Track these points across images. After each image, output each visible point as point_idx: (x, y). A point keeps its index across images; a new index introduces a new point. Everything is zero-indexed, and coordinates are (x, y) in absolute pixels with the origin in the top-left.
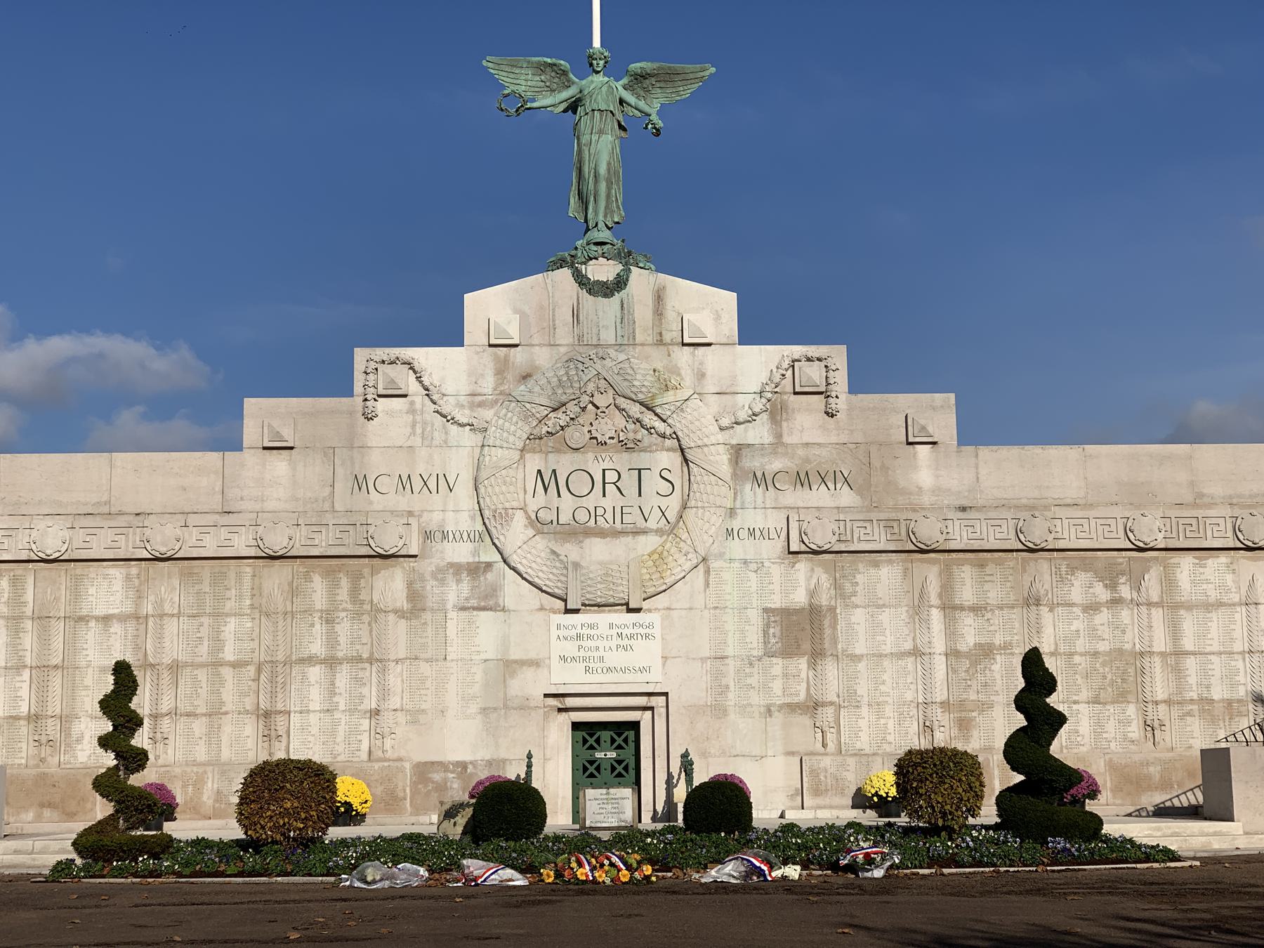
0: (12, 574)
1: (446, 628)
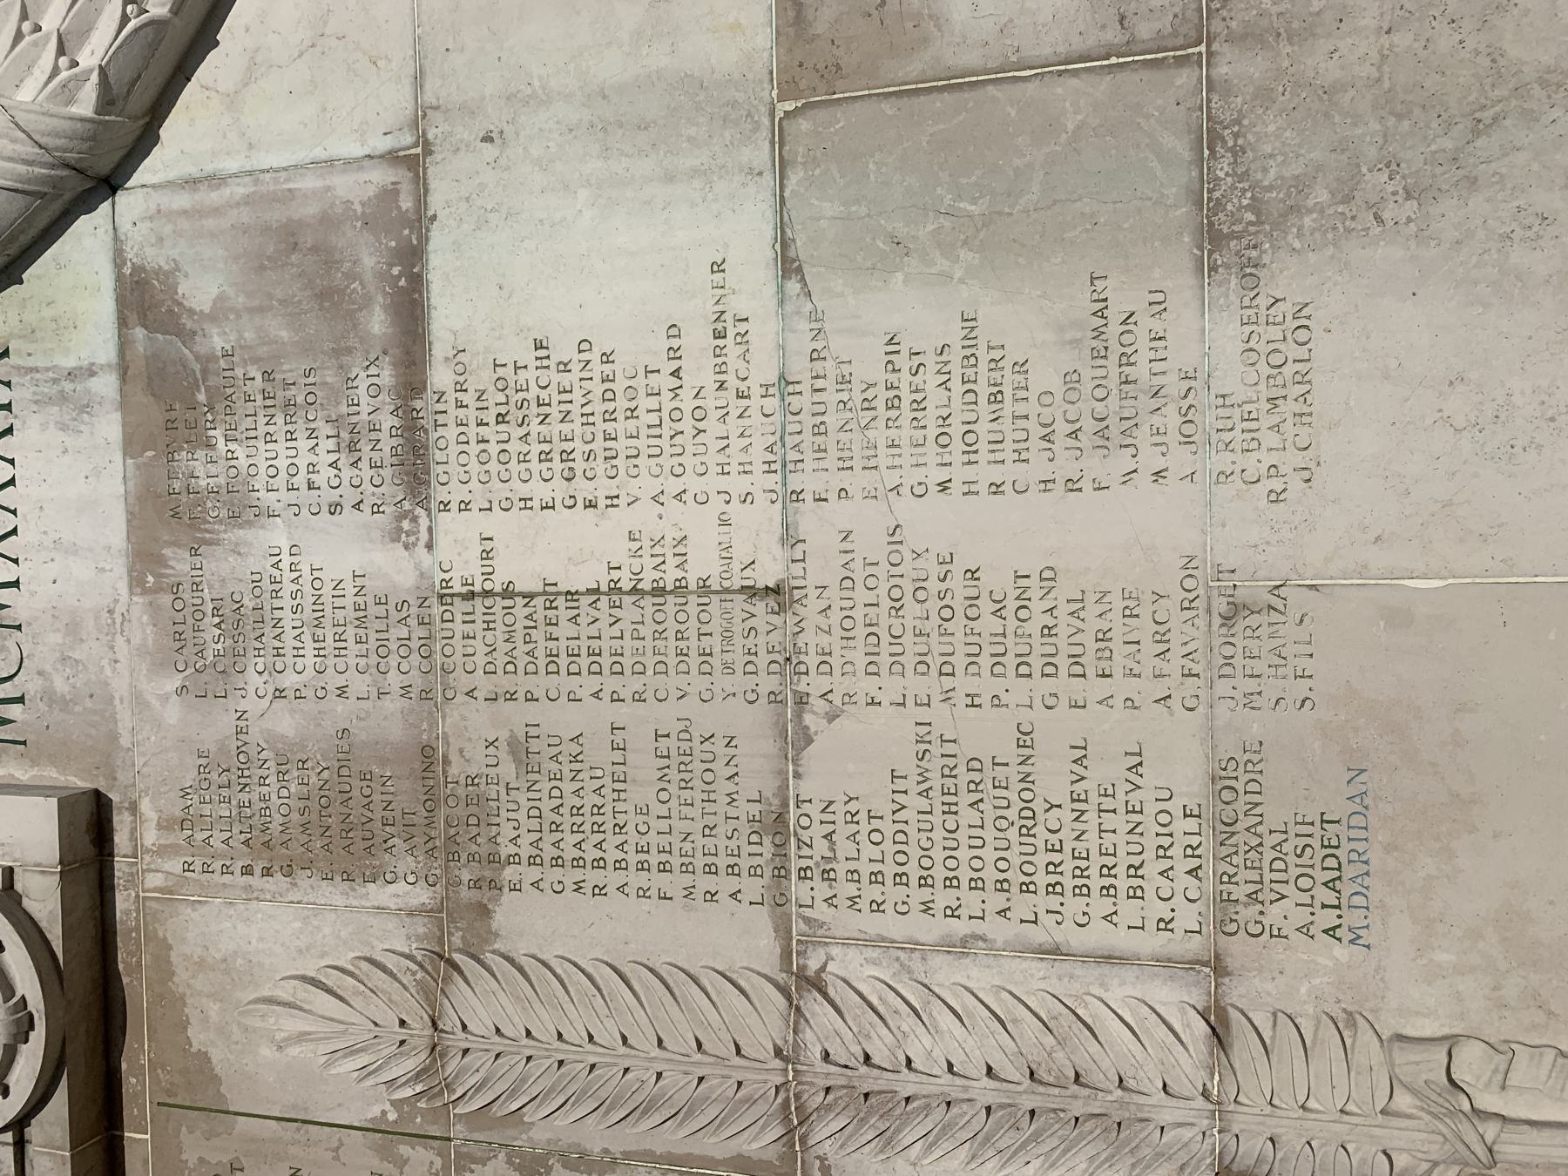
1: (550, 593)
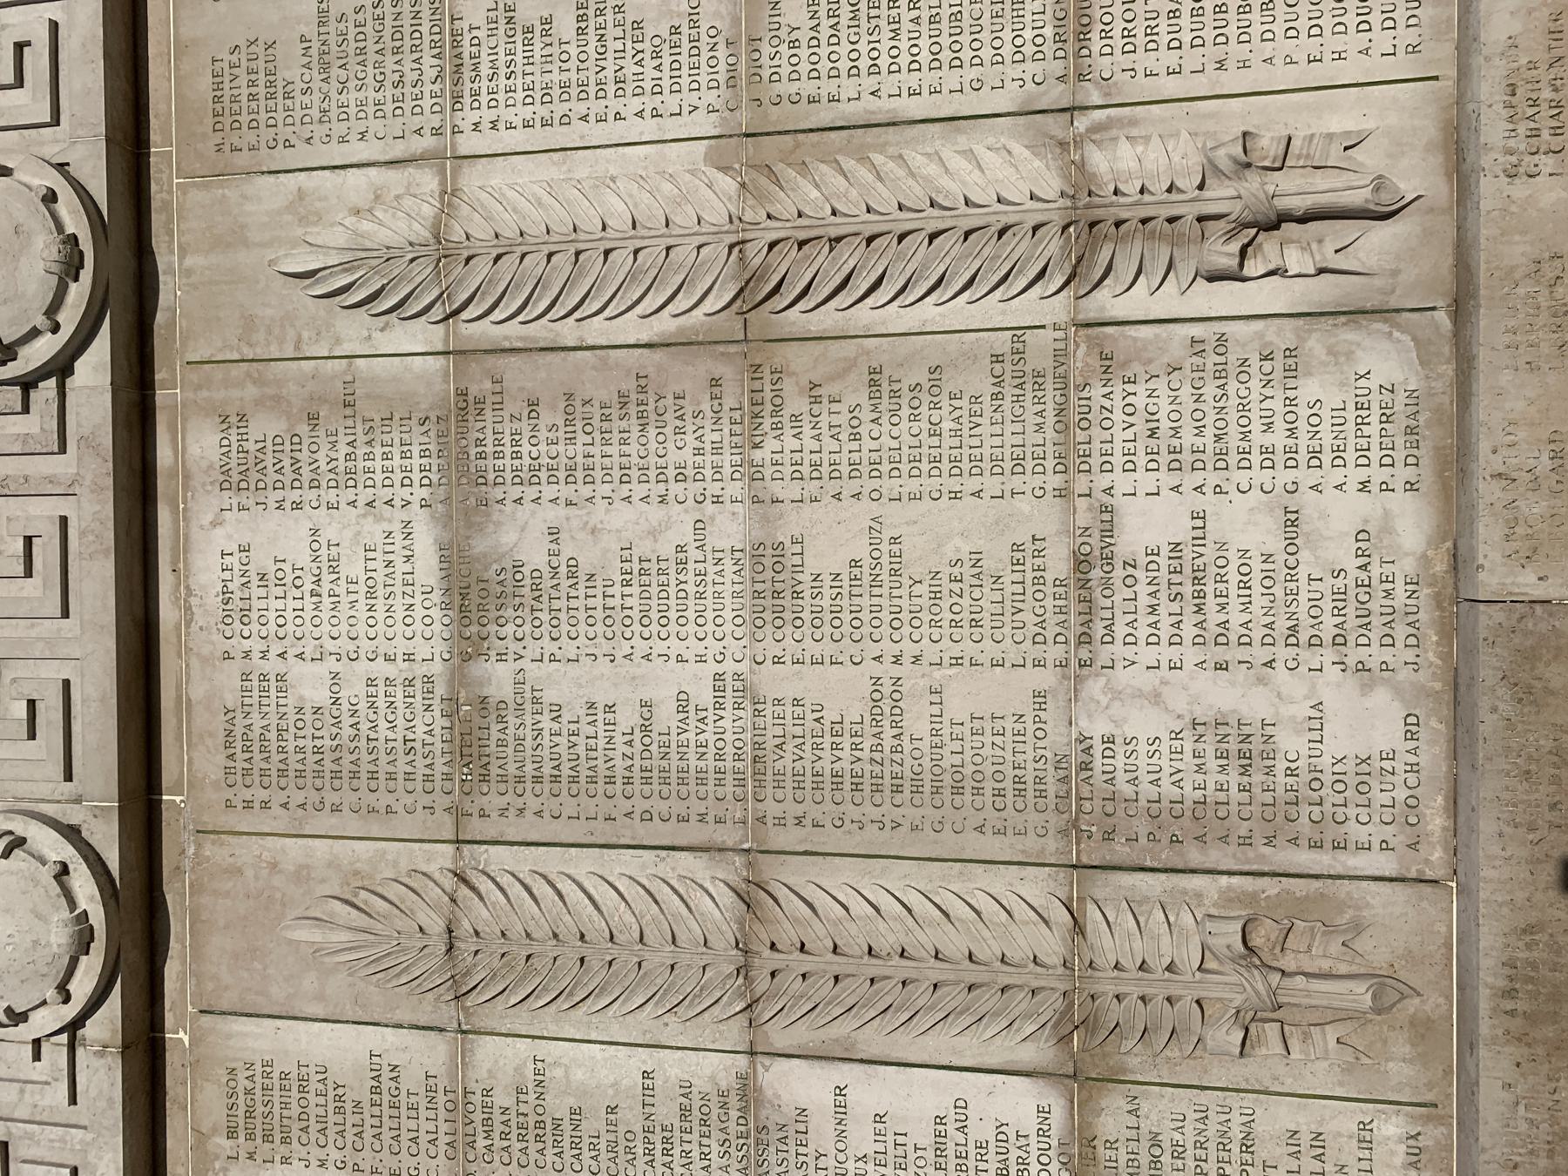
0: (222, 1143)
